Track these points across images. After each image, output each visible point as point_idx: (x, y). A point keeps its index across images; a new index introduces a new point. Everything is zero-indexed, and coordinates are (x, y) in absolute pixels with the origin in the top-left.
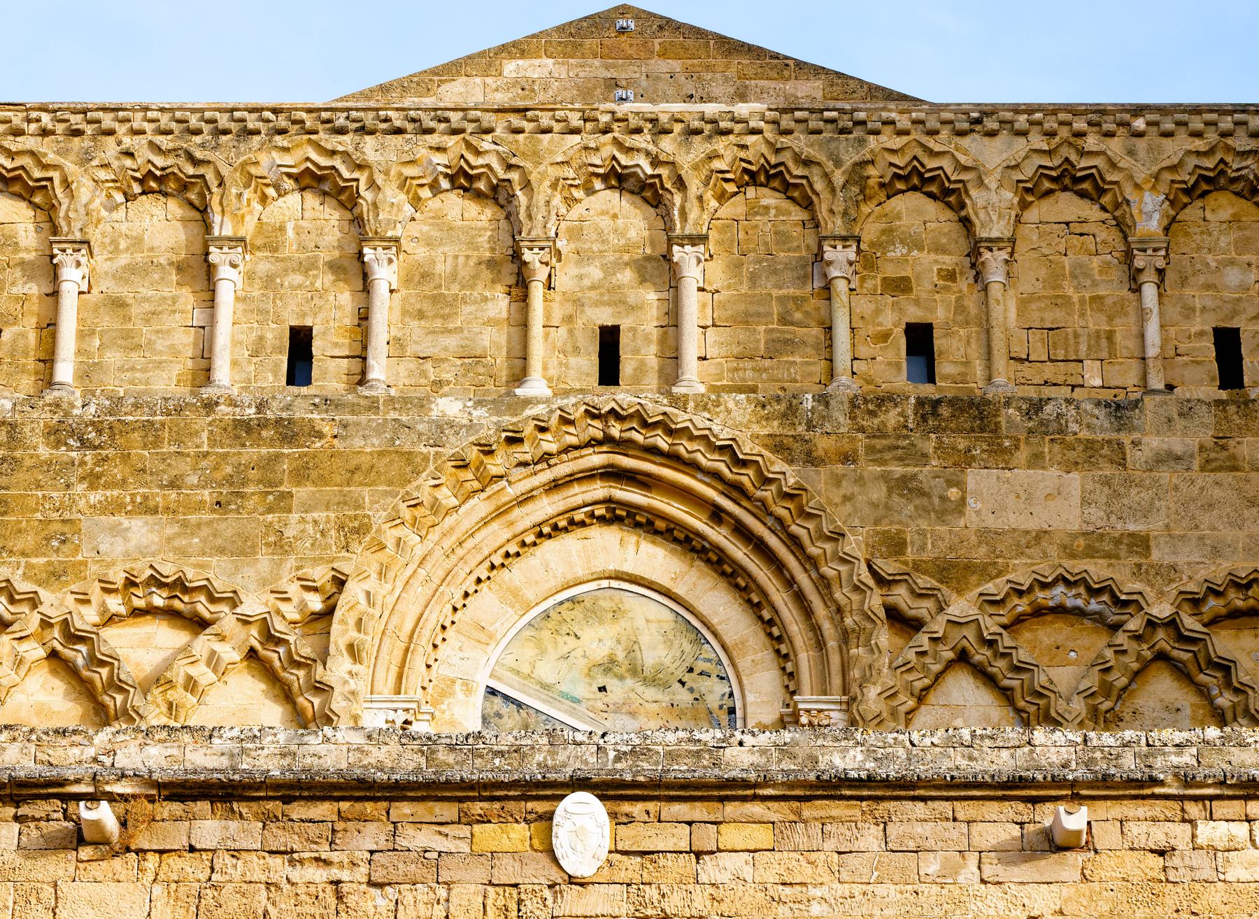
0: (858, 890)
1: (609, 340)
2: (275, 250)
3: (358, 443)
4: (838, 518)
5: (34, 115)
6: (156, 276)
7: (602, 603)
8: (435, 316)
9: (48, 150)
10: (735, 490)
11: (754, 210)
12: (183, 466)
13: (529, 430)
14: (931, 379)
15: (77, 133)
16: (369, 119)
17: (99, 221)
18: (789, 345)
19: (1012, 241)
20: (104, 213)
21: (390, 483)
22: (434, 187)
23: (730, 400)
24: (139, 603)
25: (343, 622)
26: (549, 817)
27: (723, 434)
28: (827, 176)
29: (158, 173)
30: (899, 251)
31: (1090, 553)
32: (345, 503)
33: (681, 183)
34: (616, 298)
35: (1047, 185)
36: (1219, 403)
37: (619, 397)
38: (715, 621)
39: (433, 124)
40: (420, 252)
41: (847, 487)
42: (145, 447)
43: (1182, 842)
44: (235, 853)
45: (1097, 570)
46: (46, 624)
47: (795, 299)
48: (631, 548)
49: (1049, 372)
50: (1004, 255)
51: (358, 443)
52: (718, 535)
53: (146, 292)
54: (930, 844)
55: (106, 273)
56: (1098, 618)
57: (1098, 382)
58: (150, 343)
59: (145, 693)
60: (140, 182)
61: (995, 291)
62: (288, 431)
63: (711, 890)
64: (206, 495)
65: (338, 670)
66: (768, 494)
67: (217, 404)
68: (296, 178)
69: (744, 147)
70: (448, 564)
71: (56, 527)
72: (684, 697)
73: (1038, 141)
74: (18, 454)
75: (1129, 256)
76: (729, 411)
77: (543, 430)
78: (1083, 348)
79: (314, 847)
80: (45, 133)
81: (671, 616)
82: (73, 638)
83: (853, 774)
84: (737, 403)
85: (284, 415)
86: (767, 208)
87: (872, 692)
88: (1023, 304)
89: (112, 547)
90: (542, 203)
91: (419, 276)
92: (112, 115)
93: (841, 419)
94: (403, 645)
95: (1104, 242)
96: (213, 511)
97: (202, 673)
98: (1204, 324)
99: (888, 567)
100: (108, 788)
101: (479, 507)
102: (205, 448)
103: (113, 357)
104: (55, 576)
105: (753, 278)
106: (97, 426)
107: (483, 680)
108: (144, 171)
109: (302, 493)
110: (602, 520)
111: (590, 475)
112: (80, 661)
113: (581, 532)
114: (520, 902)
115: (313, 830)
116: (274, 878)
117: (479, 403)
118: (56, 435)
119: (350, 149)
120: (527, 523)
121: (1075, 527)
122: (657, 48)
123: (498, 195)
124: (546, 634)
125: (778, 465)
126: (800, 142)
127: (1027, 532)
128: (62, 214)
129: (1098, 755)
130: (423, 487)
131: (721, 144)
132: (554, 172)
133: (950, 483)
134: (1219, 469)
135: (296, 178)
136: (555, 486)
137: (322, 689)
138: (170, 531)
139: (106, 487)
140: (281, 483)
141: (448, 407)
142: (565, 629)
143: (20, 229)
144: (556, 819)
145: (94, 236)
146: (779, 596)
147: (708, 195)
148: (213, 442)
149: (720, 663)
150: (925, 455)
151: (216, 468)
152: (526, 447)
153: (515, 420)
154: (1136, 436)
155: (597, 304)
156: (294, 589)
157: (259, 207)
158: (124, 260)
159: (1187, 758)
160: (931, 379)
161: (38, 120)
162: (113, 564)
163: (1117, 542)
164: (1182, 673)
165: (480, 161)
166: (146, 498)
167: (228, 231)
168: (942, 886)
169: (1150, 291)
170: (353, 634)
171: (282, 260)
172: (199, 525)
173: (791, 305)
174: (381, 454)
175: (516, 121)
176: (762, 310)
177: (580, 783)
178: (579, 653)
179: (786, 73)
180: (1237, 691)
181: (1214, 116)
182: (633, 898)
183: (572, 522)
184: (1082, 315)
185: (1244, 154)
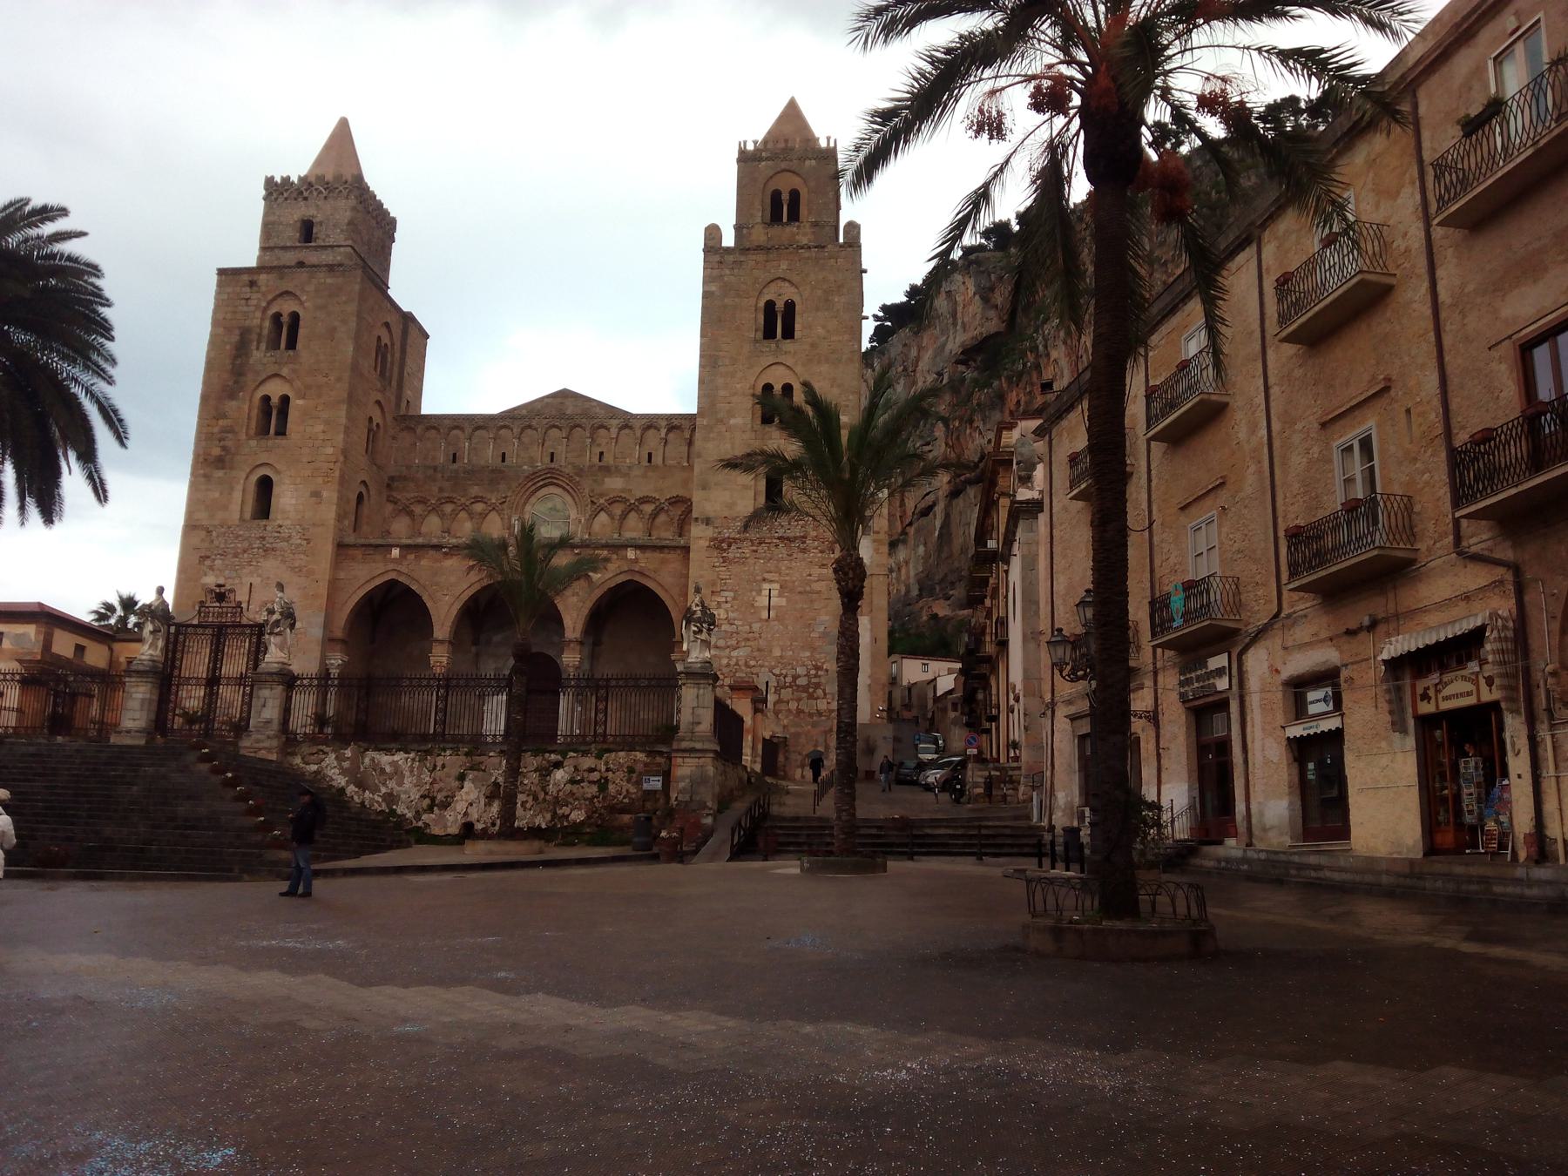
1: (552, 454)
27: (567, 472)
45: (623, 495)
52: (568, 488)
62: (501, 471)
101: (530, 484)
123: (536, 429)
141: (525, 467)
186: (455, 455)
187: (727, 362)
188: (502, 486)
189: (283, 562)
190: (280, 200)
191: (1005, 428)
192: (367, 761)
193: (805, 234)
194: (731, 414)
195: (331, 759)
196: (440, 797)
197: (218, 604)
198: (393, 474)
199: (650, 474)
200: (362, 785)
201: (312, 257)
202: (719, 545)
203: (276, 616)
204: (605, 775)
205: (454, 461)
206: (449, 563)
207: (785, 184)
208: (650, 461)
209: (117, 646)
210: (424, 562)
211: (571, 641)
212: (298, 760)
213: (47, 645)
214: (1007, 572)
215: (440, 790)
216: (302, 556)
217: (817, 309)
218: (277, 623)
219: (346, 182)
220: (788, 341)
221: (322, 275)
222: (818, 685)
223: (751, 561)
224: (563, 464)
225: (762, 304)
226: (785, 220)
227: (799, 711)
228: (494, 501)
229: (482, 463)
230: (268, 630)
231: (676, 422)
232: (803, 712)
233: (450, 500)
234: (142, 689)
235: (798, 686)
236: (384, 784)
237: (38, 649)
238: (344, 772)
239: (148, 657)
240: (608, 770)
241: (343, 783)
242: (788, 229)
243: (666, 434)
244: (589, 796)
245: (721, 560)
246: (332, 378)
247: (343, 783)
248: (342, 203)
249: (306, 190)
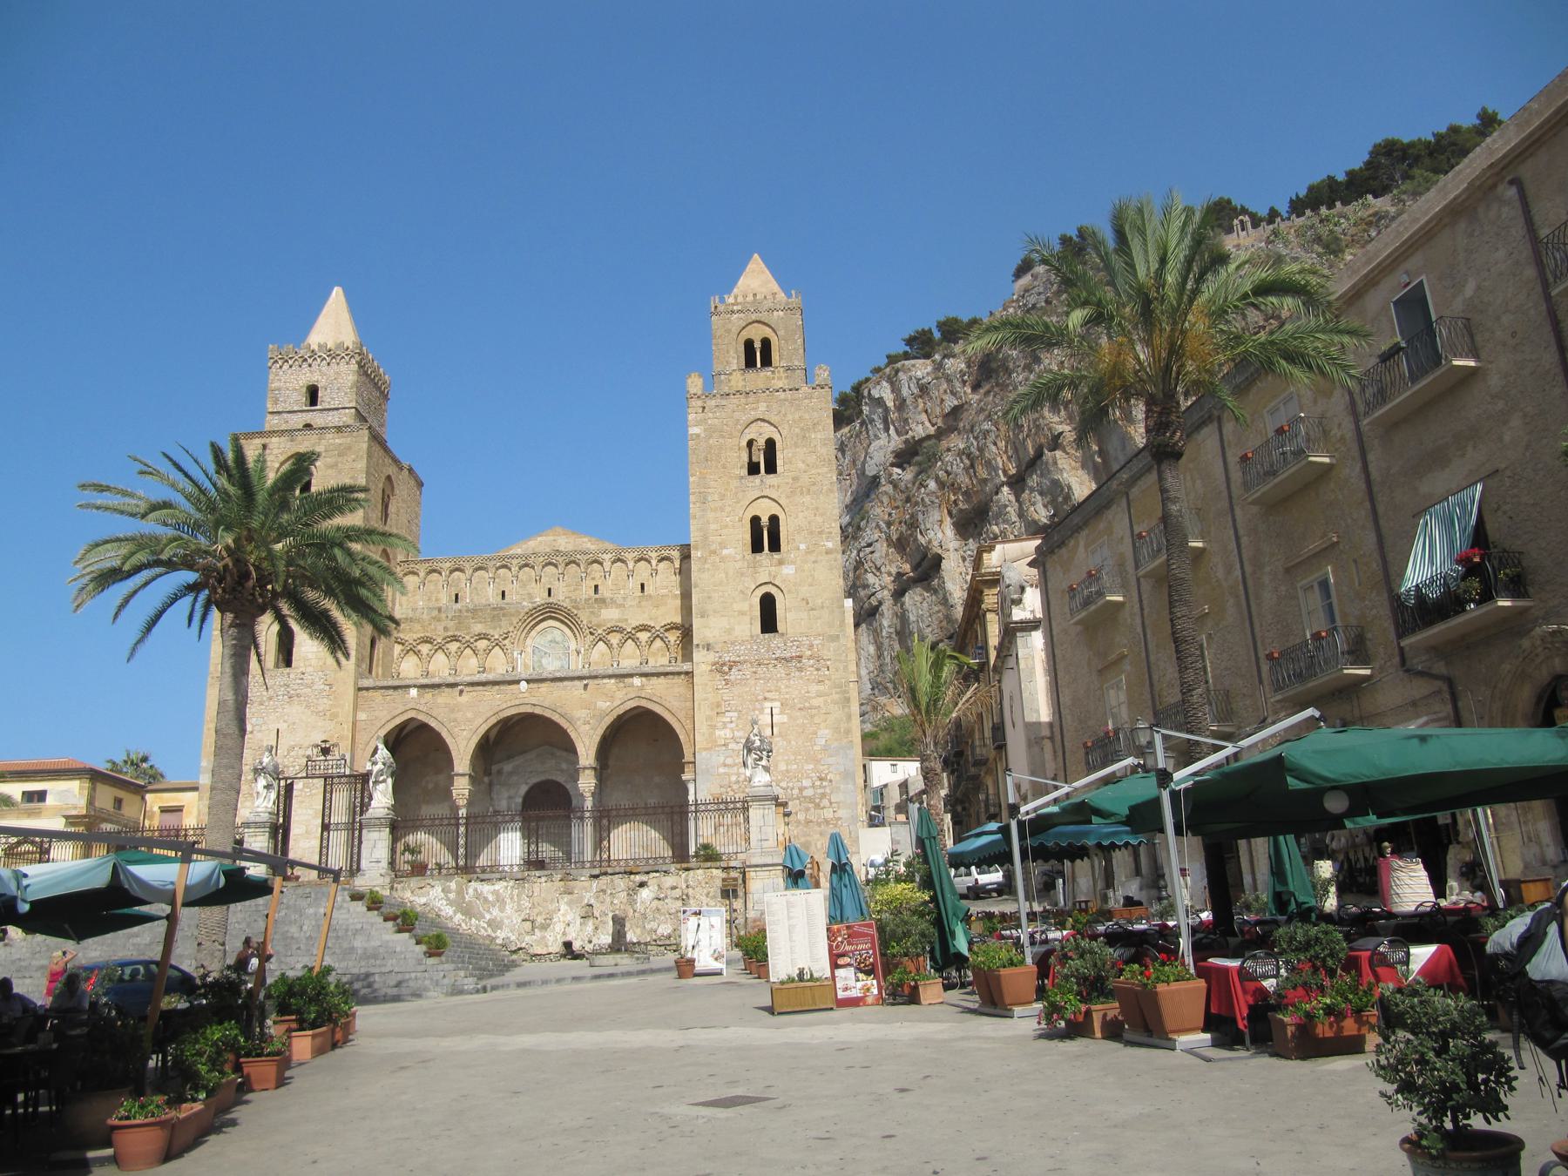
1: (550, 590)
27: (565, 605)
34: (550, 583)
45: (620, 625)
62: (502, 609)
104: (468, 634)
109: (503, 619)
118: (467, 611)
123: (533, 567)
141: (525, 603)
186: (457, 595)
187: (716, 497)
188: (504, 622)
189: (308, 707)
190: (286, 366)
191: (985, 551)
192: (471, 891)
193: (780, 378)
194: (723, 546)
195: (437, 891)
196: (540, 920)
197: (323, 758)
200: (468, 912)
201: (317, 419)
202: (721, 668)
203: (380, 766)
204: (686, 892)
205: (456, 601)
206: (465, 698)
207: (757, 334)
209: (149, 797)
211: (585, 768)
212: (408, 894)
213: (91, 802)
214: (999, 681)
215: (539, 914)
216: (325, 700)
217: (796, 445)
218: (381, 772)
219: (348, 348)
220: (772, 476)
221: (331, 436)
222: (823, 795)
223: (752, 682)
224: (561, 598)
225: (744, 443)
226: (759, 365)
227: (808, 822)
228: (497, 637)
229: (484, 602)
230: (372, 779)
231: (665, 553)
232: (811, 821)
233: (455, 639)
234: (259, 838)
235: (805, 797)
236: (488, 911)
237: (83, 802)
238: (450, 903)
239: (263, 810)
240: (687, 887)
241: (451, 913)
242: (762, 374)
244: (673, 911)
245: (724, 683)
247: (451, 913)
248: (343, 367)
249: (310, 357)
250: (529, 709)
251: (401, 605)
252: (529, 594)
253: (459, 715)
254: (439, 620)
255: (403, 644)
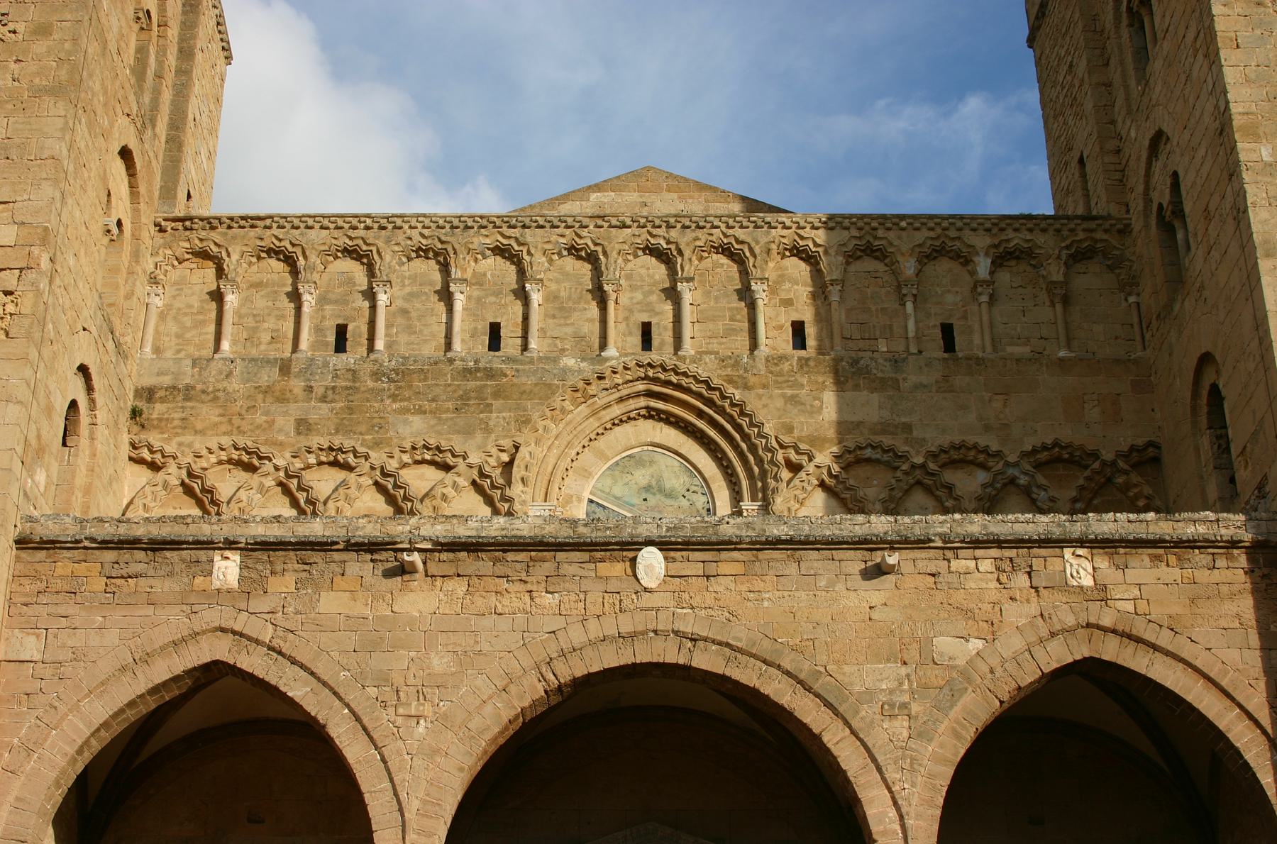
0: (786, 594)
1: (646, 330)
2: (481, 285)
3: (524, 379)
4: (760, 417)
5: (362, 219)
6: (424, 298)
7: (644, 457)
8: (561, 317)
9: (369, 235)
10: (710, 402)
11: (716, 265)
12: (438, 391)
13: (608, 373)
14: (803, 347)
15: (384, 228)
16: (527, 221)
17: (395, 271)
18: (733, 331)
19: (843, 281)
20: (397, 267)
21: (540, 399)
22: (560, 255)
23: (707, 358)
24: (419, 458)
25: (519, 467)
26: (633, 561)
27: (703, 375)
28: (751, 250)
29: (424, 248)
30: (787, 286)
31: (884, 432)
32: (519, 409)
33: (680, 253)
34: (650, 308)
35: (859, 253)
36: (944, 359)
37: (652, 357)
38: (700, 466)
39: (559, 224)
40: (554, 287)
41: (764, 400)
42: (420, 381)
43: (944, 570)
44: (479, 577)
45: (887, 441)
46: (373, 468)
47: (737, 309)
48: (659, 430)
49: (861, 344)
50: (839, 288)
51: (524, 379)
52: (701, 424)
53: (418, 305)
54: (821, 572)
55: (399, 297)
56: (887, 464)
57: (885, 349)
58: (421, 331)
59: (422, 501)
60: (416, 251)
61: (834, 305)
62: (490, 374)
63: (714, 594)
64: (450, 405)
65: (516, 490)
66: (727, 404)
67: (455, 360)
68: (492, 250)
69: (712, 235)
70: (569, 438)
71: (376, 421)
72: (685, 503)
73: (855, 233)
74: (357, 385)
75: (899, 287)
76: (706, 363)
77: (615, 373)
78: (878, 333)
79: (519, 574)
80: (367, 228)
81: (677, 464)
82: (385, 474)
83: (784, 538)
84: (710, 359)
85: (488, 366)
86: (722, 265)
87: (779, 500)
88: (848, 311)
89: (404, 431)
90: (612, 262)
91: (551, 298)
92: (401, 219)
93: (761, 367)
94: (547, 478)
95: (887, 281)
96: (454, 413)
97: (450, 491)
98: (936, 321)
99: (786, 439)
100: (417, 546)
102: (449, 382)
103: (403, 338)
104: (377, 444)
105: (717, 299)
106: (396, 371)
107: (587, 495)
108: (417, 246)
109: (497, 404)
110: (645, 417)
111: (637, 395)
112: (390, 487)
113: (633, 422)
114: (621, 601)
115: (518, 566)
116: (499, 589)
117: (583, 360)
118: (376, 376)
119: (518, 235)
120: (608, 418)
121: (876, 419)
122: (665, 187)
123: (592, 259)
124: (617, 473)
125: (730, 390)
126: (740, 234)
127: (853, 422)
128: (377, 268)
129: (902, 528)
130: (557, 402)
131: (699, 233)
132: (618, 247)
133: (815, 399)
134: (945, 391)
135: (492, 250)
136: (621, 400)
137: (509, 500)
138: (433, 422)
139: (401, 400)
140: (487, 399)
141: (569, 362)
142: (626, 470)
143: (357, 275)
144: (639, 560)
145: (393, 277)
146: (731, 454)
147: (694, 258)
148: (453, 379)
149: (702, 487)
150: (802, 385)
151: (455, 391)
152: (607, 381)
153: (601, 368)
154: (905, 375)
155: (640, 311)
156: (494, 451)
157: (472, 264)
158: (408, 290)
159: (945, 529)
160: (803, 347)
161: (365, 222)
162: (404, 439)
163: (896, 427)
164: (929, 490)
165: (582, 242)
166: (420, 406)
167: (459, 275)
168: (827, 592)
169: (909, 306)
170: (523, 473)
171: (485, 290)
172: (447, 420)
173: (735, 312)
174: (536, 385)
175: (600, 222)
176: (721, 314)
177: (649, 542)
178: (633, 482)
179: (729, 200)
180: (955, 499)
181: (939, 220)
182: (677, 598)
183: (629, 418)
184: (877, 317)
185: (954, 239)
186: (341, 332)
188: (500, 417)
198: (148, 381)
199: (960, 381)
208: (949, 345)
210: (331, 603)
231: (1016, 239)
243: (992, 273)
246: (20, 27)
250: (670, 653)
251: (157, 350)
252: (579, 338)
253: (399, 662)
254: (282, 399)
255: (154, 467)
